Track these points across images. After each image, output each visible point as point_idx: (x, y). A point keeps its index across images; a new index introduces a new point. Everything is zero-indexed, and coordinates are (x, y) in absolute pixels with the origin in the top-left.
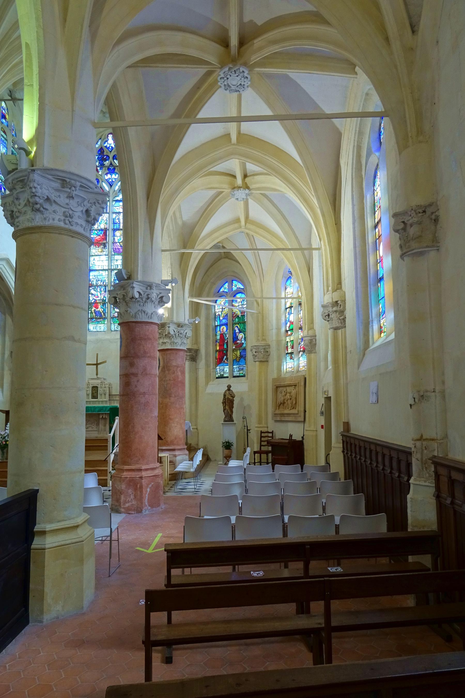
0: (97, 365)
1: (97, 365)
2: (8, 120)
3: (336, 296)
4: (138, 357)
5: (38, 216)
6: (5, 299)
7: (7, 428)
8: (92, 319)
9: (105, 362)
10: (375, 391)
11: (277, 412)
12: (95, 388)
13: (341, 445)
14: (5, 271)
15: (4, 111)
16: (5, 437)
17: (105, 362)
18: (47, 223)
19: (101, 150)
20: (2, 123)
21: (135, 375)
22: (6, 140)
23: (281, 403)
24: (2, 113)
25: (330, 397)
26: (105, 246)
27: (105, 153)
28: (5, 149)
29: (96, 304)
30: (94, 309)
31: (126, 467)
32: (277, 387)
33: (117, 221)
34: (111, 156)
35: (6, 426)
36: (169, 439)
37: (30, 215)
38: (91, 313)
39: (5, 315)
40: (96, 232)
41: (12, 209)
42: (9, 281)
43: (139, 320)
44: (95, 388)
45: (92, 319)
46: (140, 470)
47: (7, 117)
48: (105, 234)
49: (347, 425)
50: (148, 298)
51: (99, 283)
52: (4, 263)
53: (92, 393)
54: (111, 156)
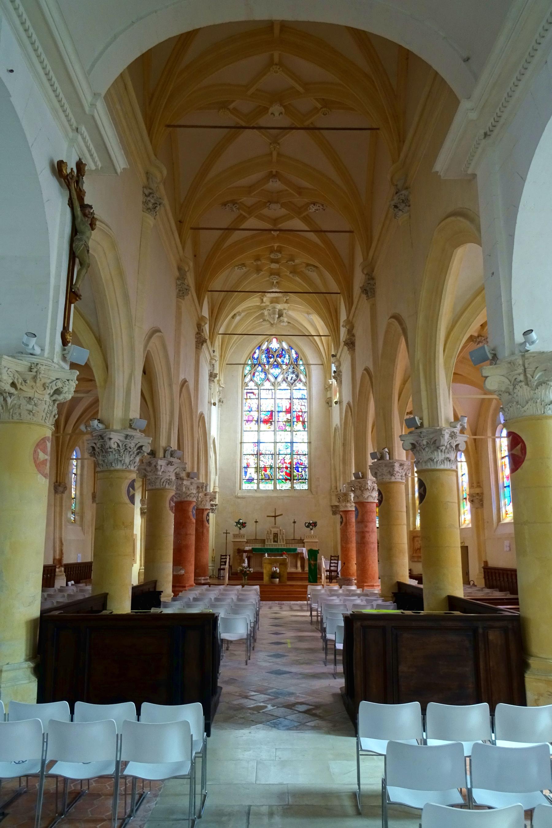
0: (275, 517)
1: (275, 517)
3: (478, 490)
4: (369, 522)
5: (393, 477)
8: (262, 479)
9: (281, 515)
10: (508, 545)
11: (415, 555)
12: (276, 535)
13: (483, 575)
17: (281, 515)
18: (396, 480)
19: (268, 350)
21: (368, 532)
23: (418, 549)
25: (467, 547)
26: (271, 424)
27: (271, 353)
29: (265, 469)
30: (263, 472)
31: (365, 584)
32: (414, 537)
33: (280, 405)
34: (275, 356)
36: (351, 573)
37: (389, 476)
38: (262, 475)
40: (264, 413)
43: (369, 501)
44: (276, 535)
45: (262, 479)
46: (373, 586)
48: (271, 415)
49: (486, 563)
50: (373, 489)
51: (267, 453)
53: (274, 538)
54: (275, 356)
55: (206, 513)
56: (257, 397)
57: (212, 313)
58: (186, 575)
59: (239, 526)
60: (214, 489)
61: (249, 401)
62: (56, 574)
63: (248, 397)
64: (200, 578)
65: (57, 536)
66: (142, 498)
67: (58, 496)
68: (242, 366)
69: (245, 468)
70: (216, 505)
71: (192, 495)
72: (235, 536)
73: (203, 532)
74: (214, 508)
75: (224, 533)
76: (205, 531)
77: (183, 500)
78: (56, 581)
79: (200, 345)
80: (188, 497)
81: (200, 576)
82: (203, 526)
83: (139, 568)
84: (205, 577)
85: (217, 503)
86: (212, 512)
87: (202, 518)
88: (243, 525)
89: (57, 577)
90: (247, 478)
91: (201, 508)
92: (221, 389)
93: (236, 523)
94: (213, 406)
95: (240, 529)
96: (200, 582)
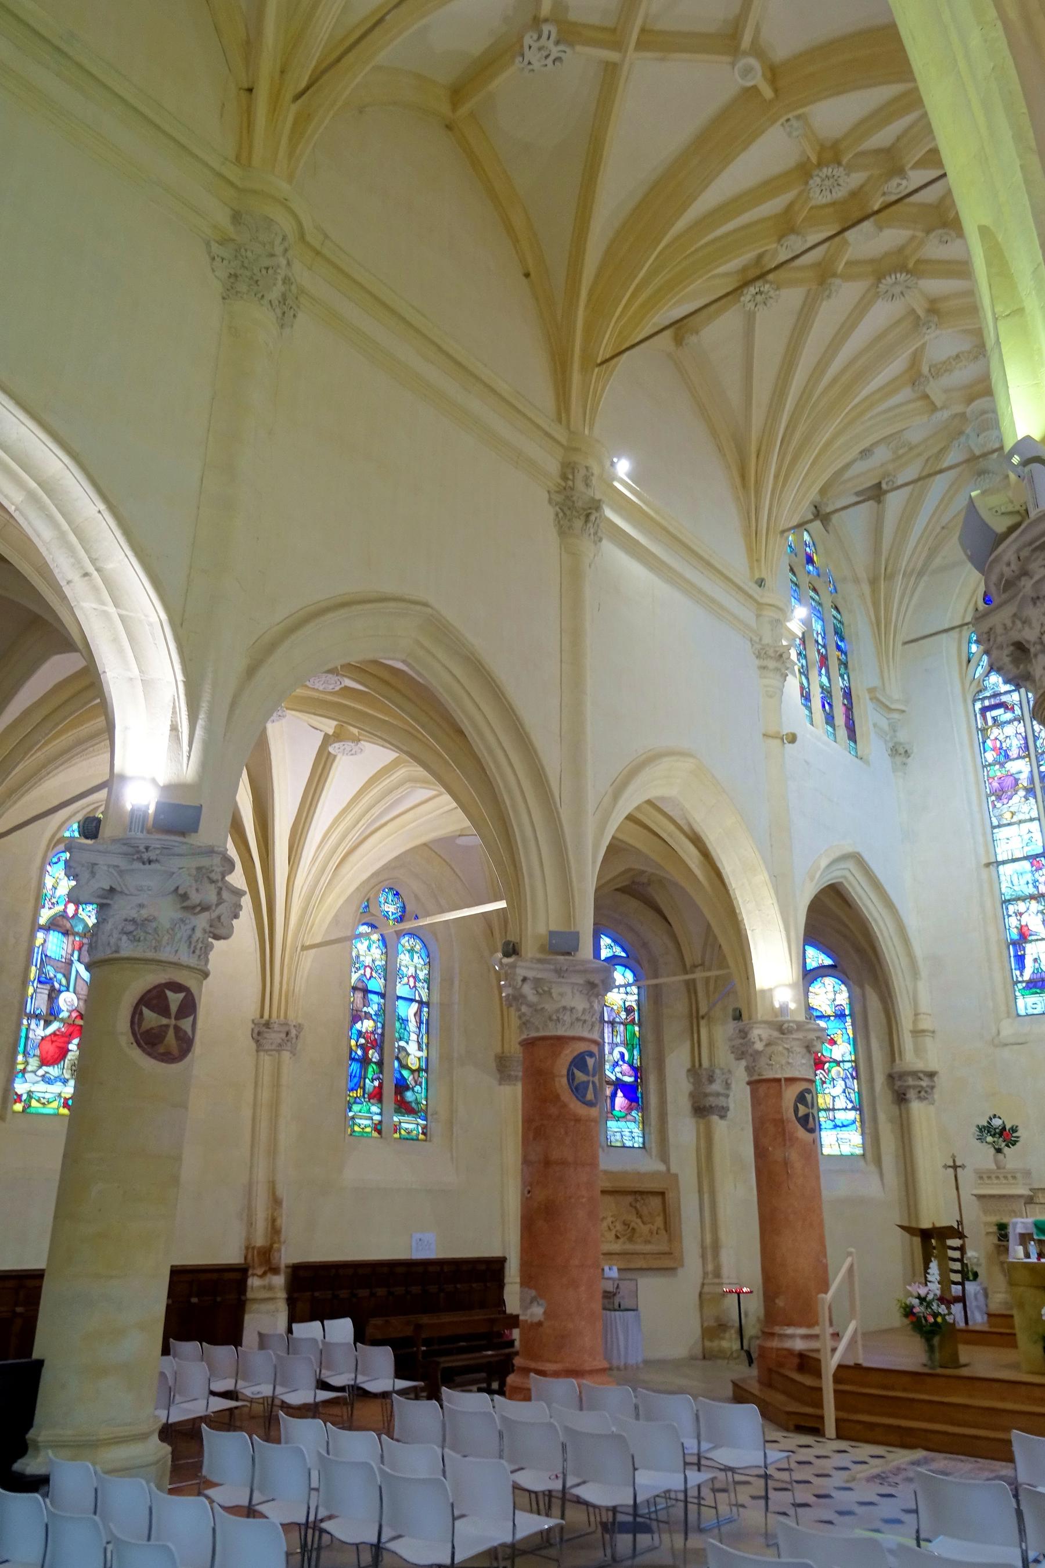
2: (817, 565)
6: (859, 950)
7: (929, 1278)
14: (855, 883)
15: (808, 549)
16: (929, 1305)
20: (809, 573)
22: (820, 604)
24: (807, 554)
28: (820, 622)
35: (926, 1272)
39: (862, 987)
41: (1015, 636)
42: (864, 905)
47: (815, 559)
52: (850, 865)
55: (790, 1094)
56: (1018, 711)
57: (743, 477)
58: (546, 1324)
59: (990, 1139)
60: (915, 1022)
61: (995, 732)
62: (250, 1295)
63: (990, 722)
64: (790, 1331)
65: (261, 1174)
66: (693, 1065)
67: (266, 1060)
68: (954, 634)
69: (1014, 943)
70: (931, 1075)
71: (567, 1018)
72: (982, 1176)
73: (786, 1163)
74: (924, 1084)
75: (946, 1167)
76: (794, 1155)
77: (534, 1034)
78: (248, 1318)
79: (578, 523)
80: (551, 1024)
81: (789, 1324)
82: (784, 1140)
83: (699, 1281)
84: (810, 1325)
85: (932, 1066)
86: (920, 1099)
87: (779, 1111)
88: (1003, 1136)
89: (249, 1307)
90: (1027, 975)
91: (769, 1074)
92: (896, 716)
93: (981, 1129)
94: (788, 746)
95: (999, 1151)
96: (788, 1344)
